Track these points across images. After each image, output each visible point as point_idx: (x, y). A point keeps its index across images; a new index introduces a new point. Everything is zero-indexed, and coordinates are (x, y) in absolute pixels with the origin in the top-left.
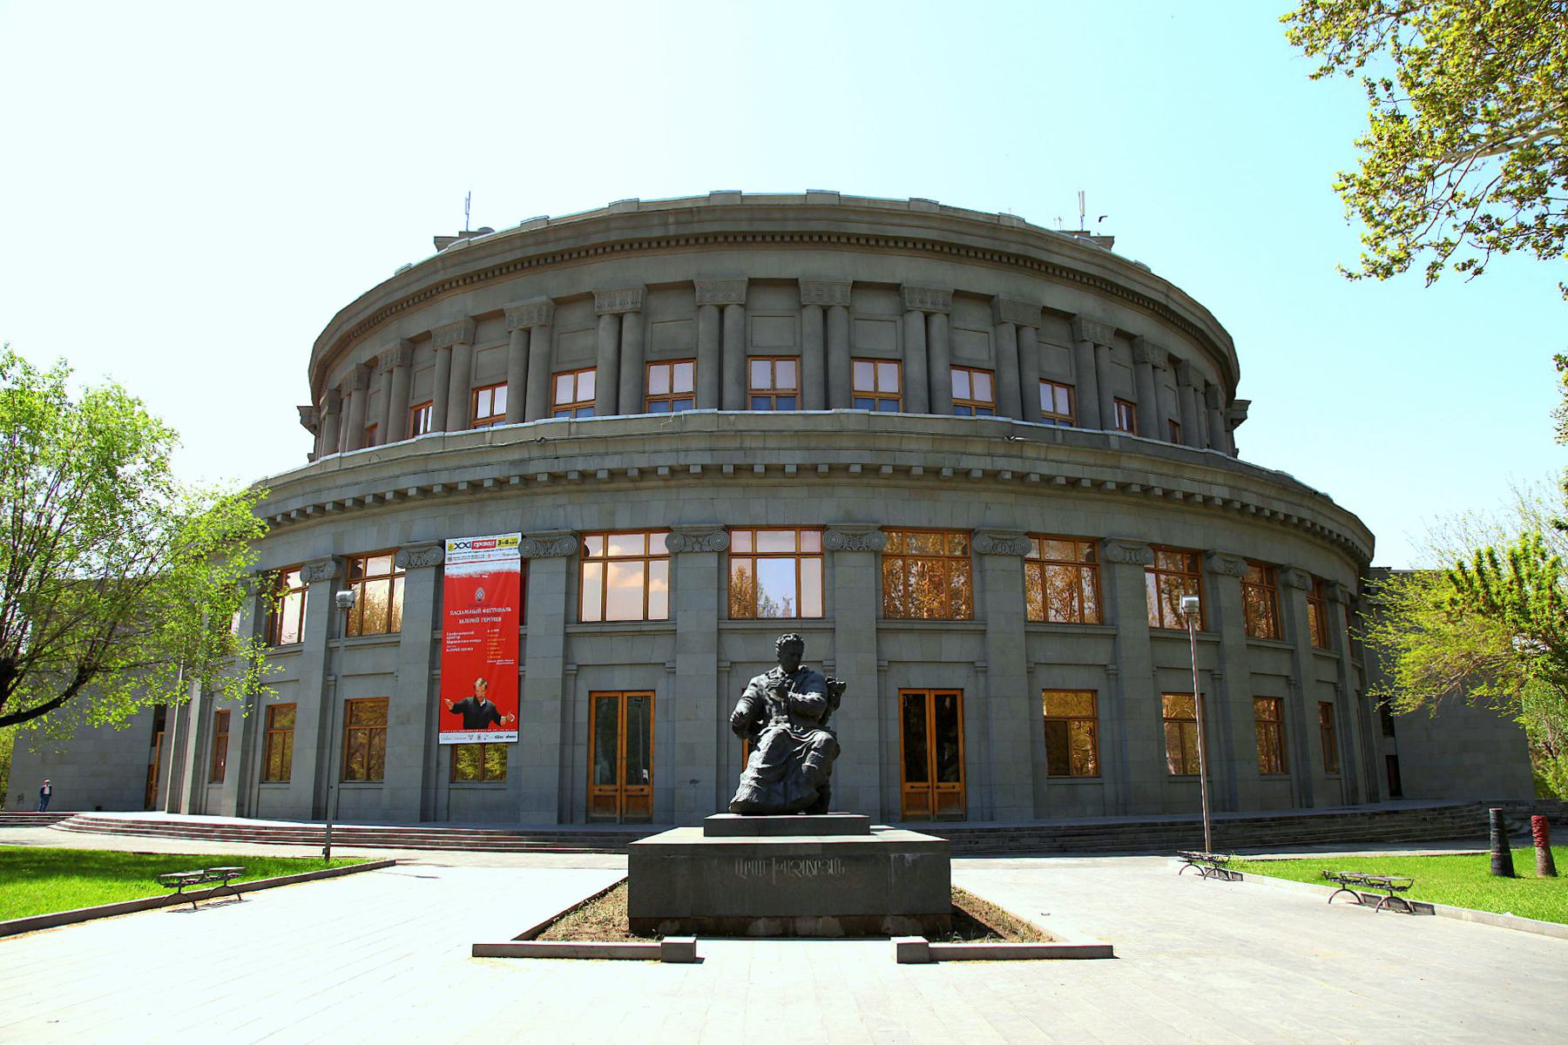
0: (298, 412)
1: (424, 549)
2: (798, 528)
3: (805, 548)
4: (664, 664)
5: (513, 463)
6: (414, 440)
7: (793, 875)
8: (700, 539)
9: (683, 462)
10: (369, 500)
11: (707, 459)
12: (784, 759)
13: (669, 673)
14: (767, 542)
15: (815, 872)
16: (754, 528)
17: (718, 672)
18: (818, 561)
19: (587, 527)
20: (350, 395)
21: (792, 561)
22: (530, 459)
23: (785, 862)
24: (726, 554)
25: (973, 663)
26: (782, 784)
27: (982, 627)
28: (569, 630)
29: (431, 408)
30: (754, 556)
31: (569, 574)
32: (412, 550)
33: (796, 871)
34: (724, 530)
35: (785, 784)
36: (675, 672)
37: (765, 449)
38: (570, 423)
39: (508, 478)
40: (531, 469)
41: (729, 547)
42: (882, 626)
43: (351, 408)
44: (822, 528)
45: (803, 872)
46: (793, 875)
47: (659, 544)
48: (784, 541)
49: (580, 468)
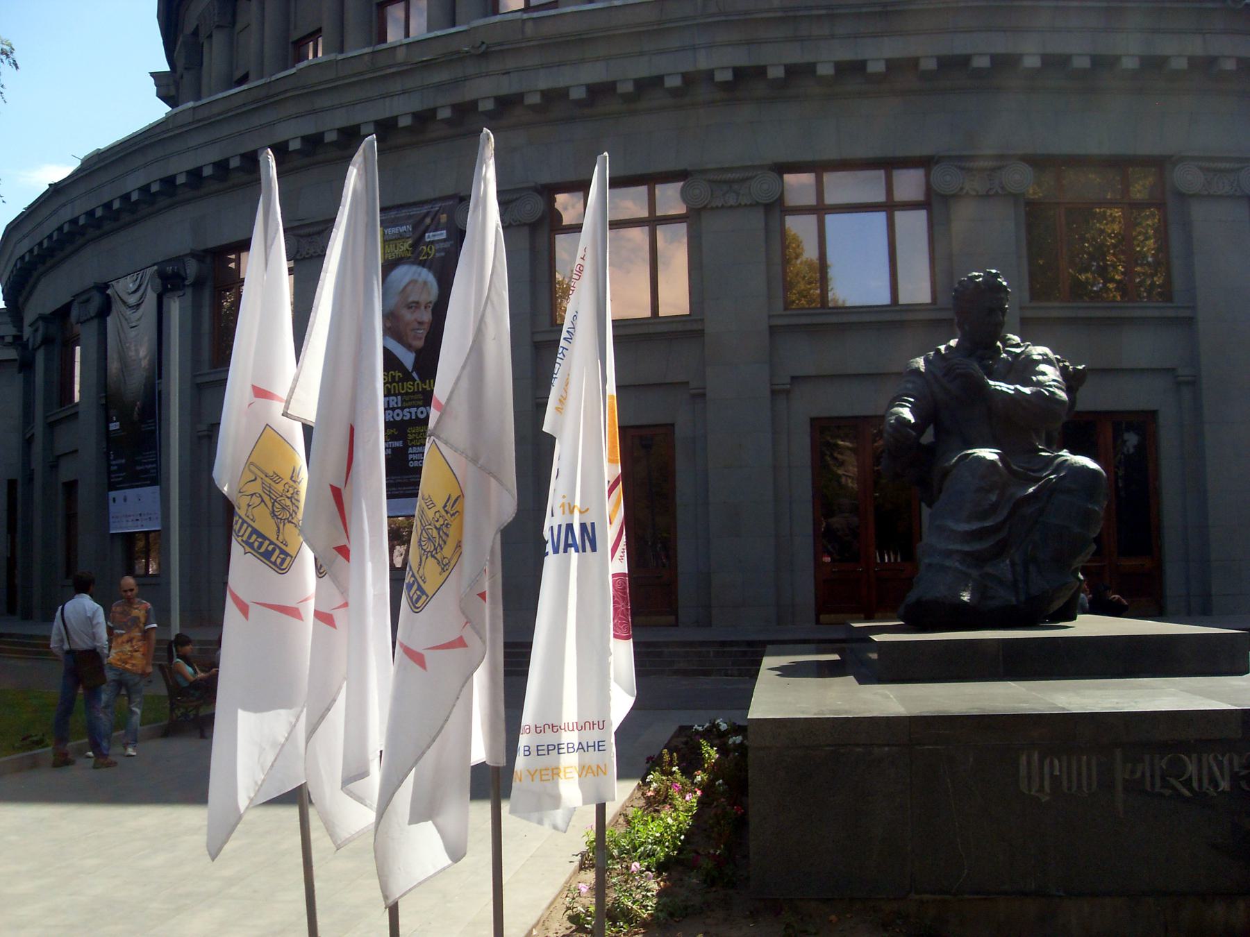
0: (152, 80)
1: (316, 229)
2: (889, 164)
3: (901, 195)
4: (687, 383)
5: (439, 87)
6: (293, 71)
7: (1168, 792)
8: (736, 187)
9: (703, 63)
10: (235, 163)
11: (741, 58)
12: (1005, 512)
13: (694, 396)
14: (841, 188)
15: (1224, 785)
16: (818, 168)
17: (773, 392)
18: (922, 215)
19: (558, 178)
20: (210, 36)
21: (880, 218)
22: (466, 79)
23: (1147, 758)
24: (777, 208)
25: (1171, 371)
26: (1008, 562)
27: (1187, 313)
28: (539, 338)
29: (320, 40)
30: (820, 210)
31: (533, 250)
32: (302, 232)
33: (1173, 781)
34: (773, 170)
35: (1013, 564)
36: (703, 395)
37: (833, 36)
38: (524, 21)
39: (433, 111)
40: (471, 91)
41: (781, 199)
42: (1029, 314)
43: (215, 57)
44: (924, 163)
45: (1195, 785)
46: (1168, 792)
47: (670, 199)
48: (868, 187)
49: (543, 85)
